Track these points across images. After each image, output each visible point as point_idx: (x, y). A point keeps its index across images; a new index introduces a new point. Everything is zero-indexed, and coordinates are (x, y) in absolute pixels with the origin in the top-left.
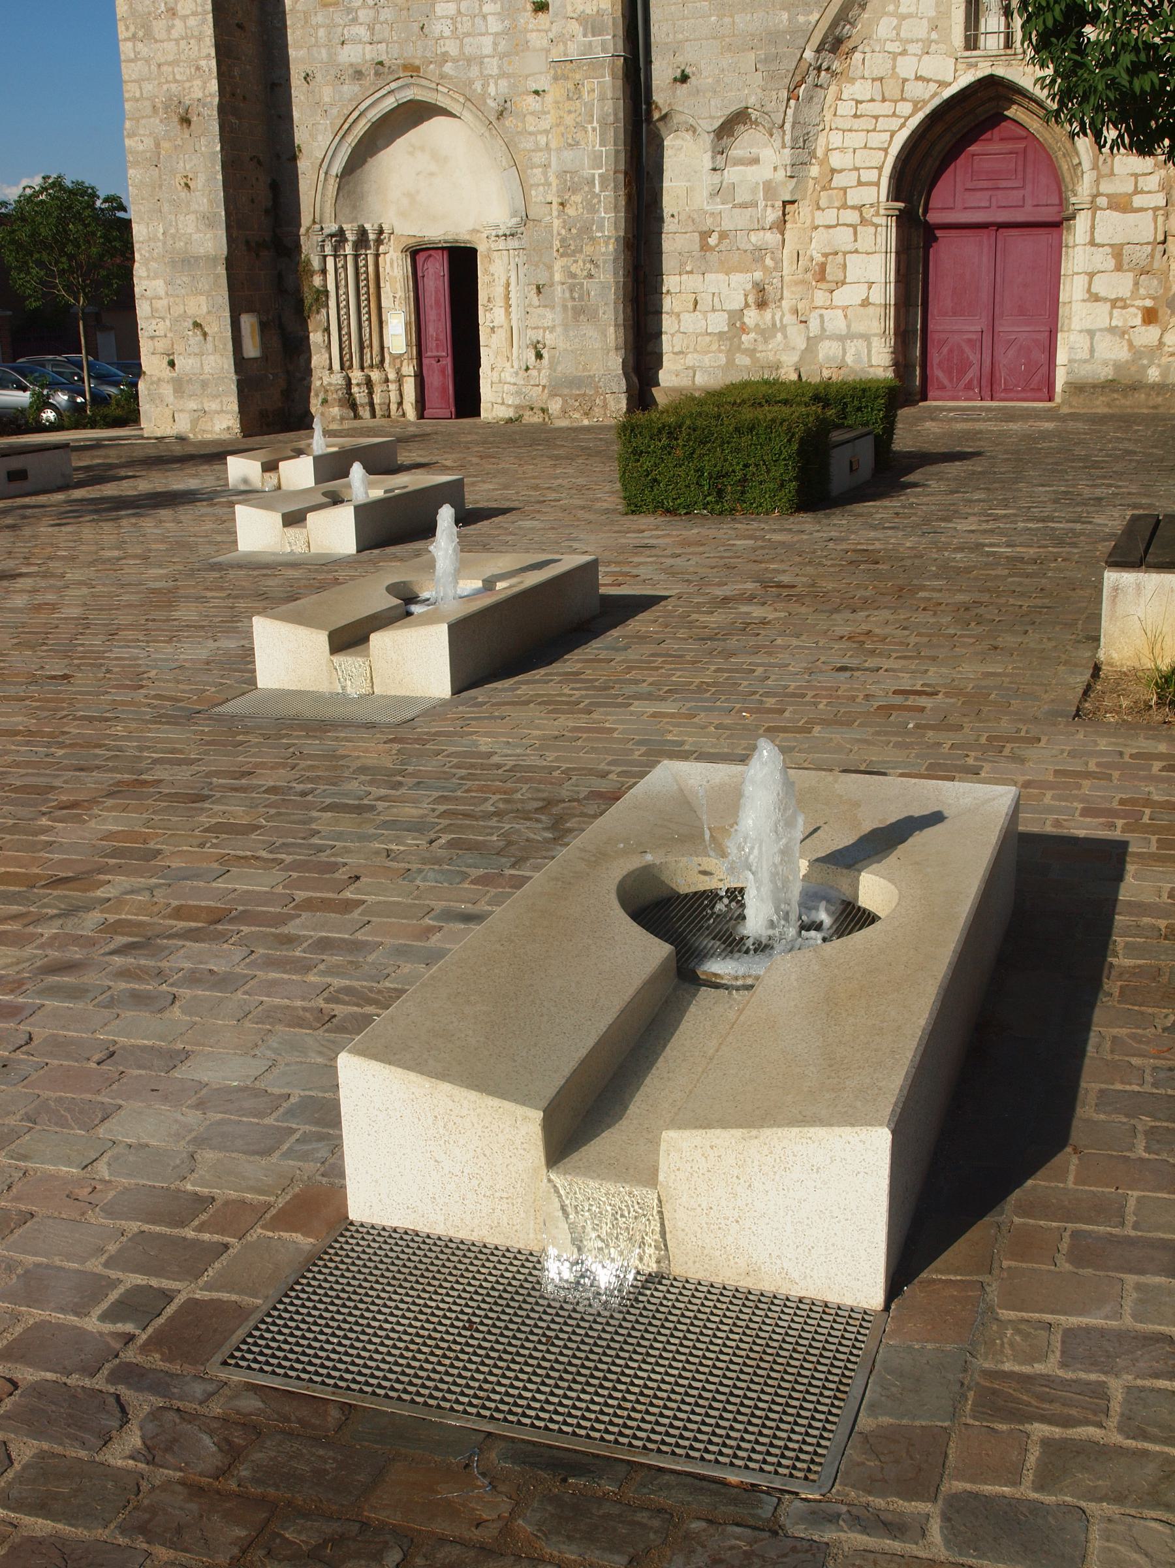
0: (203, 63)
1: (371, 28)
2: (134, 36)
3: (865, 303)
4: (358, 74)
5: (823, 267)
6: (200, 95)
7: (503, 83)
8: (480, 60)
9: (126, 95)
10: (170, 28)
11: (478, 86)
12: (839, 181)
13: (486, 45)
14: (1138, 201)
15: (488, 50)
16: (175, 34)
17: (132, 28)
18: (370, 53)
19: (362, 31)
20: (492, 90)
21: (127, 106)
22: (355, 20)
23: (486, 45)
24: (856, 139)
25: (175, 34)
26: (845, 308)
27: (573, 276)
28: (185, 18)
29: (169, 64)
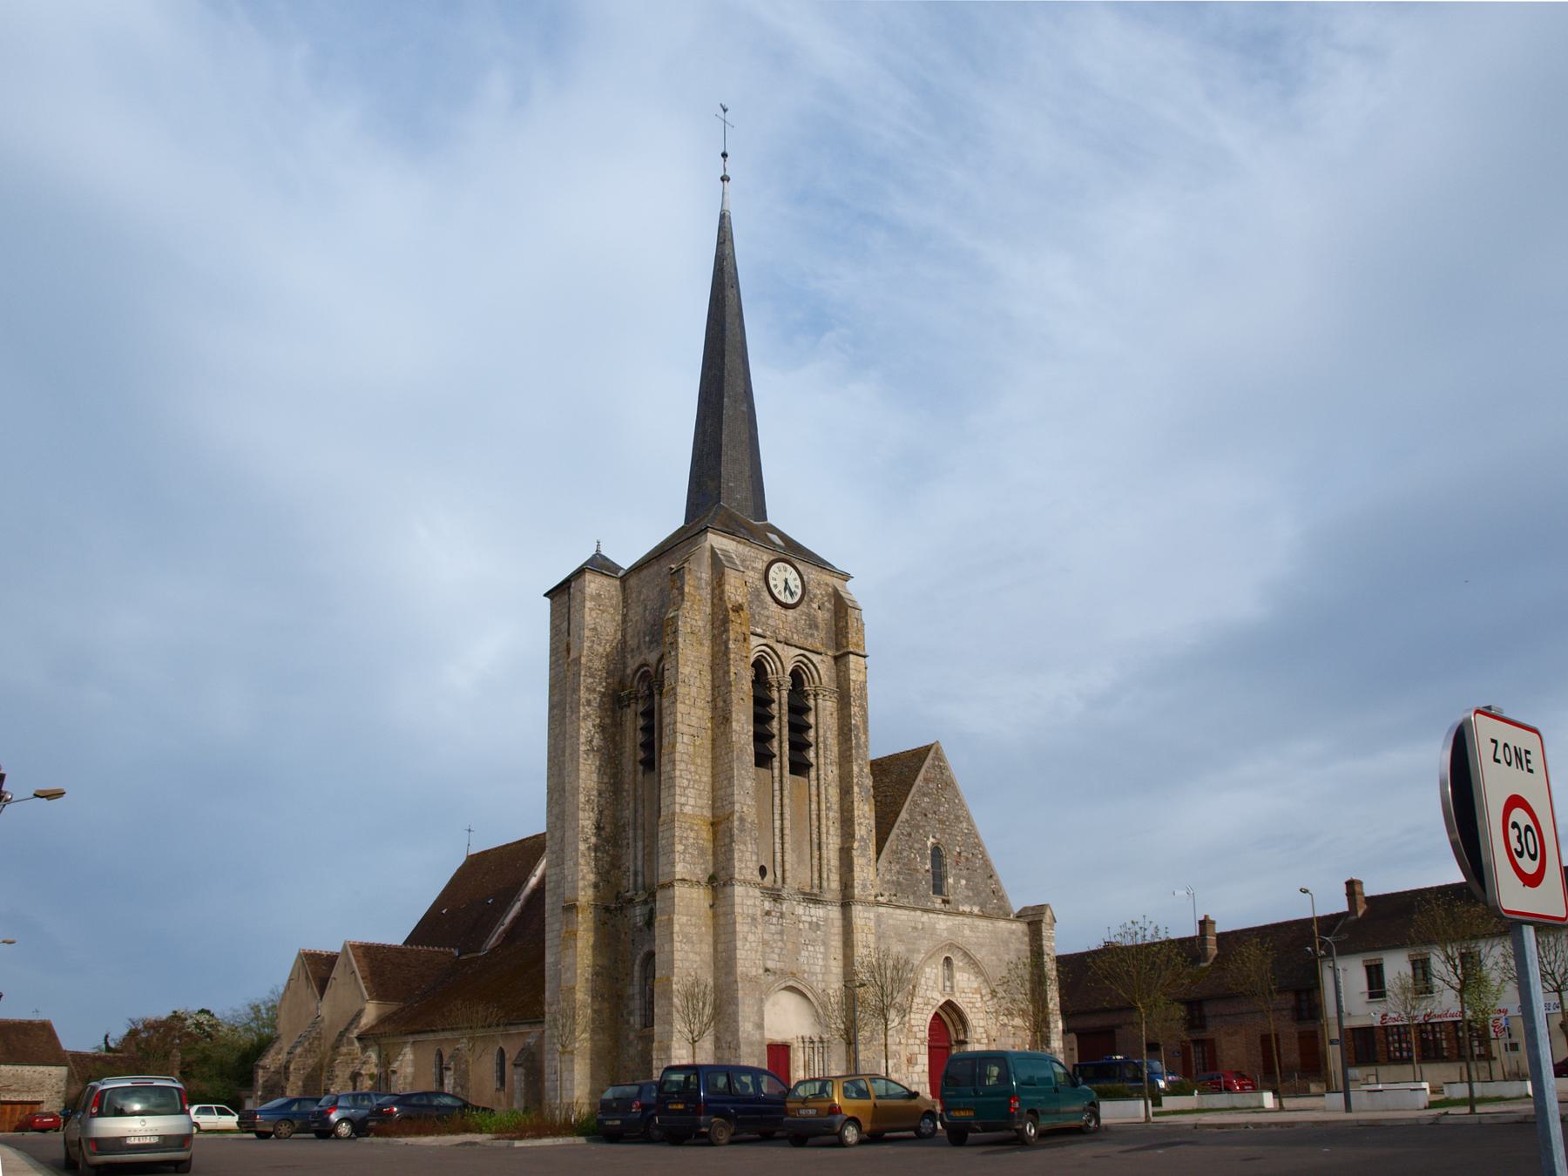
0: (757, 962)
1: (779, 955)
2: (681, 942)
3: (923, 1071)
4: (775, 973)
5: (911, 1058)
6: (755, 974)
7: (823, 984)
8: (816, 974)
9: (675, 966)
10: (744, 945)
11: (815, 984)
12: (915, 1029)
13: (818, 969)
14: (983, 1041)
15: (818, 971)
16: (746, 948)
17: (681, 937)
18: (780, 965)
19: (776, 957)
20: (819, 986)
21: (676, 970)
22: (773, 952)
23: (818, 969)
24: (918, 1016)
25: (746, 948)
26: (918, 1073)
27: (868, 1058)
28: (750, 942)
29: (743, 959)
